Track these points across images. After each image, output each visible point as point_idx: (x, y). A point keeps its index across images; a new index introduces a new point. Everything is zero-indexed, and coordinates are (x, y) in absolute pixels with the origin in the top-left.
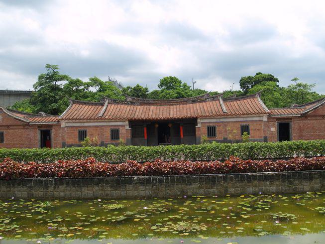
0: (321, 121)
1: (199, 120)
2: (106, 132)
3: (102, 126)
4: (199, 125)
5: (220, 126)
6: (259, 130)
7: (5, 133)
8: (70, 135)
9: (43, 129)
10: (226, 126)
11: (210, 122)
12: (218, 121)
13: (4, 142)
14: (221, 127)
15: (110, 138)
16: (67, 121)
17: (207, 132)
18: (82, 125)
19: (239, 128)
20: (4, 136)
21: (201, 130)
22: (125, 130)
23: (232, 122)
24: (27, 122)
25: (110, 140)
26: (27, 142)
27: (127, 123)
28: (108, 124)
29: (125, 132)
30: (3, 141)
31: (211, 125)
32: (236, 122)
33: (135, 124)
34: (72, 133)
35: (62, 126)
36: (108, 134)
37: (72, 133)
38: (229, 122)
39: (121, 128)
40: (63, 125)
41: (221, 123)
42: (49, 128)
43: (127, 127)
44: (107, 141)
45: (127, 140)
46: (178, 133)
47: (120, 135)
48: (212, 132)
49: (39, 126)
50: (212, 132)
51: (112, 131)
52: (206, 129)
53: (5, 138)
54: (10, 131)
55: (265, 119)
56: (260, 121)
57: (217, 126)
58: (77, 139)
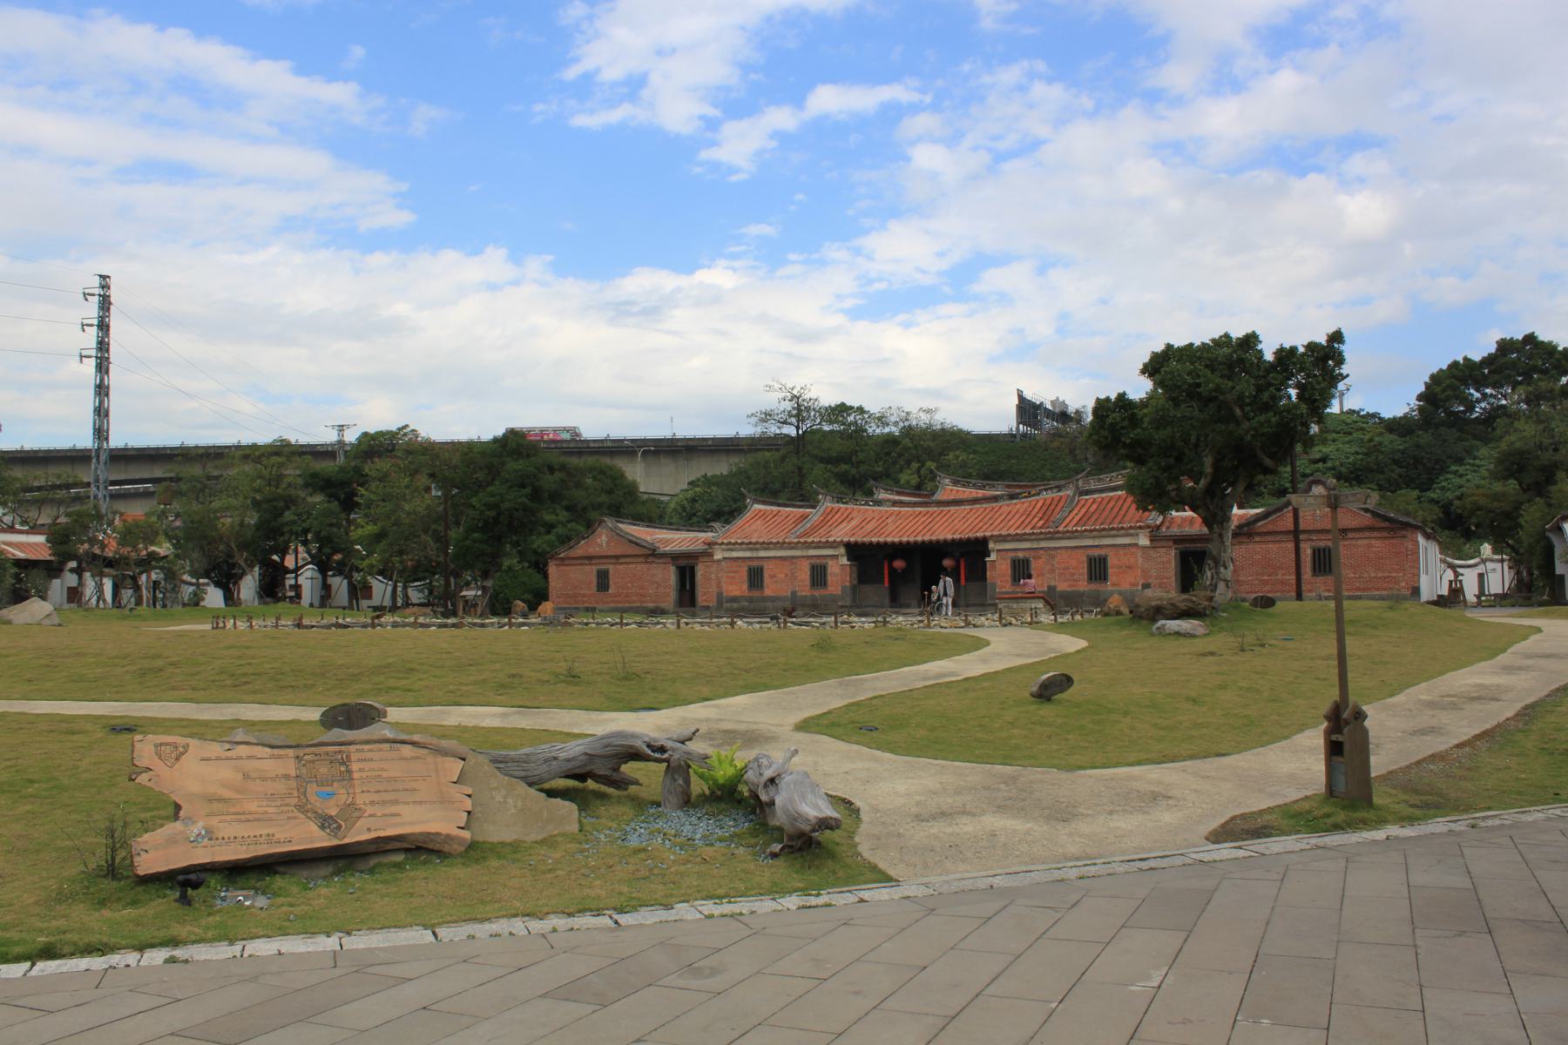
1: (991, 545)
3: (793, 557)
4: (993, 557)
5: (1040, 558)
6: (1130, 567)
7: (611, 570)
9: (683, 562)
10: (1053, 557)
12: (1035, 545)
13: (610, 591)
14: (1042, 560)
15: (808, 583)
16: (723, 547)
18: (754, 554)
19: (1083, 562)
20: (611, 576)
21: (998, 566)
22: (840, 568)
23: (1067, 548)
24: (650, 549)
25: (808, 588)
26: (651, 591)
27: (842, 550)
28: (805, 553)
30: (608, 587)
31: (1021, 555)
33: (856, 551)
35: (716, 557)
36: (804, 574)
37: (736, 572)
38: (1058, 548)
39: (830, 562)
40: (718, 556)
41: (1042, 552)
43: (844, 561)
44: (802, 591)
45: (844, 588)
47: (829, 578)
50: (1021, 569)
51: (813, 568)
52: (1009, 566)
53: (611, 582)
54: (621, 567)
55: (1144, 541)
56: (1130, 545)
57: (1034, 557)
58: (745, 586)
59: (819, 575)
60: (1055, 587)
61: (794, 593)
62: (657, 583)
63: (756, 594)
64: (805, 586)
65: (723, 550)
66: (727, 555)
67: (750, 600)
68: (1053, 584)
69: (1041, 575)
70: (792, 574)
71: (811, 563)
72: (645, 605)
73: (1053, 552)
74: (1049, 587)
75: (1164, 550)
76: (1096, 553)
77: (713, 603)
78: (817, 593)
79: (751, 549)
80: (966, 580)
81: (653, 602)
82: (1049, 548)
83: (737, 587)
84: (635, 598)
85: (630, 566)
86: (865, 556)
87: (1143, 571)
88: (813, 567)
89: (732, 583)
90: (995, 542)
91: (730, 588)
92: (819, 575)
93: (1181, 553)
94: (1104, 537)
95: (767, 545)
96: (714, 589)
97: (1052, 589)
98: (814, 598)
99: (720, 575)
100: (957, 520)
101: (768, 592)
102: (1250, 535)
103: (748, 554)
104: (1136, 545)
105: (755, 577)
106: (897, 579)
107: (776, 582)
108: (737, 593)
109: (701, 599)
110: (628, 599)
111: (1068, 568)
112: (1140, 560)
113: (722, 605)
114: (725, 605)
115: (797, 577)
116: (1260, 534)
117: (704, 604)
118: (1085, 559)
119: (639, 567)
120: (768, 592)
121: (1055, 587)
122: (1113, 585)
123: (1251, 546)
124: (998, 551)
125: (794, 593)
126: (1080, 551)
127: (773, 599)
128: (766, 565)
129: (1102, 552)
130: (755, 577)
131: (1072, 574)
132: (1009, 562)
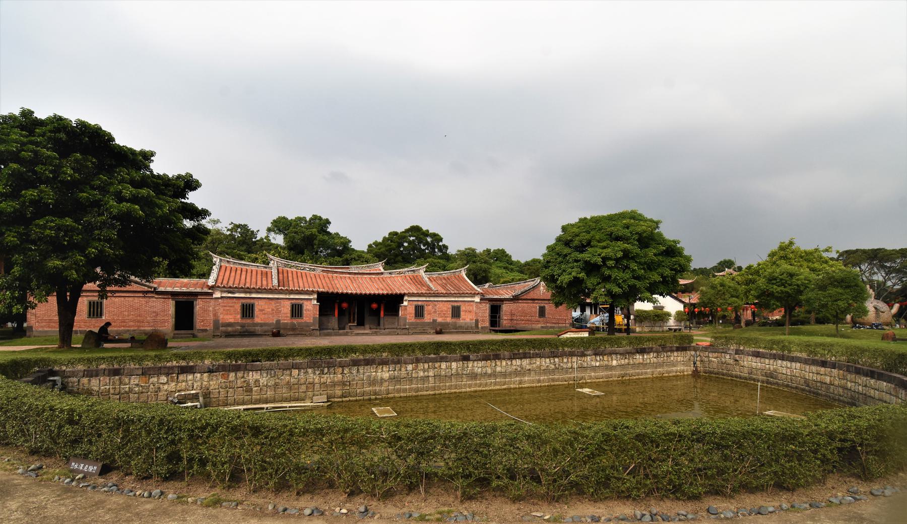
0: (532, 305)
1: (406, 298)
2: (283, 307)
3: (278, 299)
4: (405, 303)
6: (470, 312)
8: (228, 310)
9: (181, 298)
11: (418, 301)
13: (104, 318)
14: (431, 307)
15: (289, 315)
17: (414, 312)
18: (248, 295)
21: (408, 309)
22: (311, 307)
27: (316, 296)
28: (287, 297)
29: (312, 309)
30: (101, 315)
31: (420, 303)
32: (447, 301)
34: (231, 306)
35: (214, 296)
36: (286, 308)
37: (231, 306)
38: (439, 301)
42: (191, 298)
43: (315, 302)
44: (284, 320)
46: (376, 313)
47: (304, 312)
48: (419, 311)
49: (173, 294)
50: (419, 311)
52: (414, 308)
53: (104, 311)
54: (117, 299)
55: (477, 299)
56: (471, 301)
58: (239, 316)
59: (297, 310)
60: (436, 320)
61: (278, 321)
62: (155, 312)
63: (249, 321)
64: (287, 317)
65: (222, 292)
66: (224, 295)
67: (243, 326)
68: (435, 318)
69: (430, 314)
70: (277, 309)
71: (291, 303)
72: (142, 329)
73: (436, 303)
74: (433, 320)
75: (484, 304)
76: (456, 304)
77: (210, 327)
78: (296, 321)
79: (246, 292)
80: (385, 315)
81: (151, 326)
82: (435, 301)
83: (232, 316)
84: (132, 324)
85: (126, 299)
86: (328, 301)
87: (476, 313)
88: (293, 305)
89: (227, 314)
90: (408, 296)
91: (226, 317)
92: (297, 310)
93: (491, 306)
94: (466, 297)
95: (258, 291)
96: (212, 317)
97: (434, 321)
98: (294, 324)
99: (217, 308)
100: (328, 282)
101: (257, 320)
102: (518, 300)
103: (242, 295)
104: (473, 301)
105: (248, 310)
106: (342, 313)
107: (264, 314)
108: (232, 321)
109: (199, 323)
110: (123, 324)
111: (442, 311)
112: (475, 308)
113: (218, 328)
114: (221, 328)
115: (280, 311)
116: (521, 299)
117: (202, 328)
118: (450, 306)
119: (136, 300)
120: (257, 320)
121: (436, 320)
122: (462, 320)
123: (518, 304)
124: (409, 301)
125: (278, 321)
126: (448, 303)
127: (261, 325)
128: (256, 302)
129: (458, 304)
130: (248, 310)
131: (444, 314)
132: (414, 307)
